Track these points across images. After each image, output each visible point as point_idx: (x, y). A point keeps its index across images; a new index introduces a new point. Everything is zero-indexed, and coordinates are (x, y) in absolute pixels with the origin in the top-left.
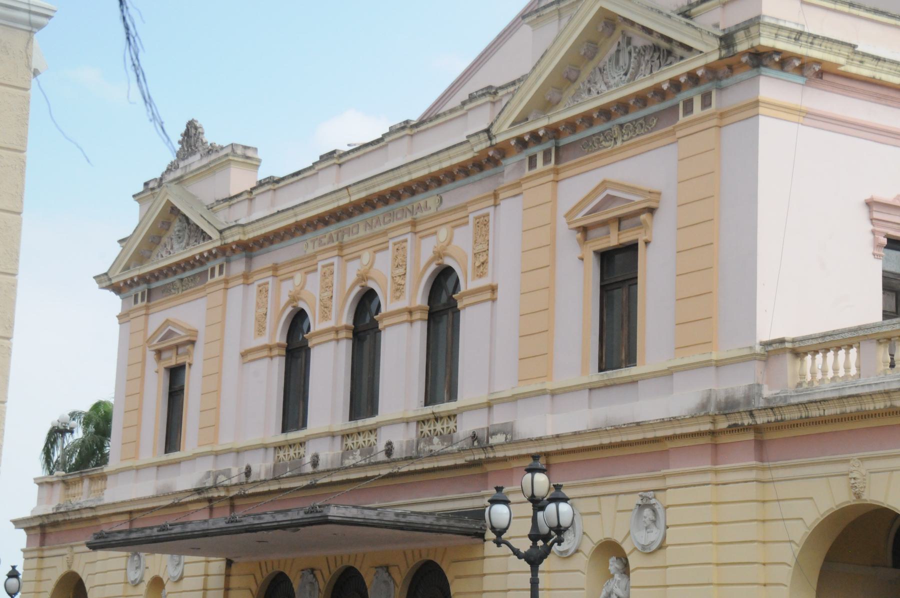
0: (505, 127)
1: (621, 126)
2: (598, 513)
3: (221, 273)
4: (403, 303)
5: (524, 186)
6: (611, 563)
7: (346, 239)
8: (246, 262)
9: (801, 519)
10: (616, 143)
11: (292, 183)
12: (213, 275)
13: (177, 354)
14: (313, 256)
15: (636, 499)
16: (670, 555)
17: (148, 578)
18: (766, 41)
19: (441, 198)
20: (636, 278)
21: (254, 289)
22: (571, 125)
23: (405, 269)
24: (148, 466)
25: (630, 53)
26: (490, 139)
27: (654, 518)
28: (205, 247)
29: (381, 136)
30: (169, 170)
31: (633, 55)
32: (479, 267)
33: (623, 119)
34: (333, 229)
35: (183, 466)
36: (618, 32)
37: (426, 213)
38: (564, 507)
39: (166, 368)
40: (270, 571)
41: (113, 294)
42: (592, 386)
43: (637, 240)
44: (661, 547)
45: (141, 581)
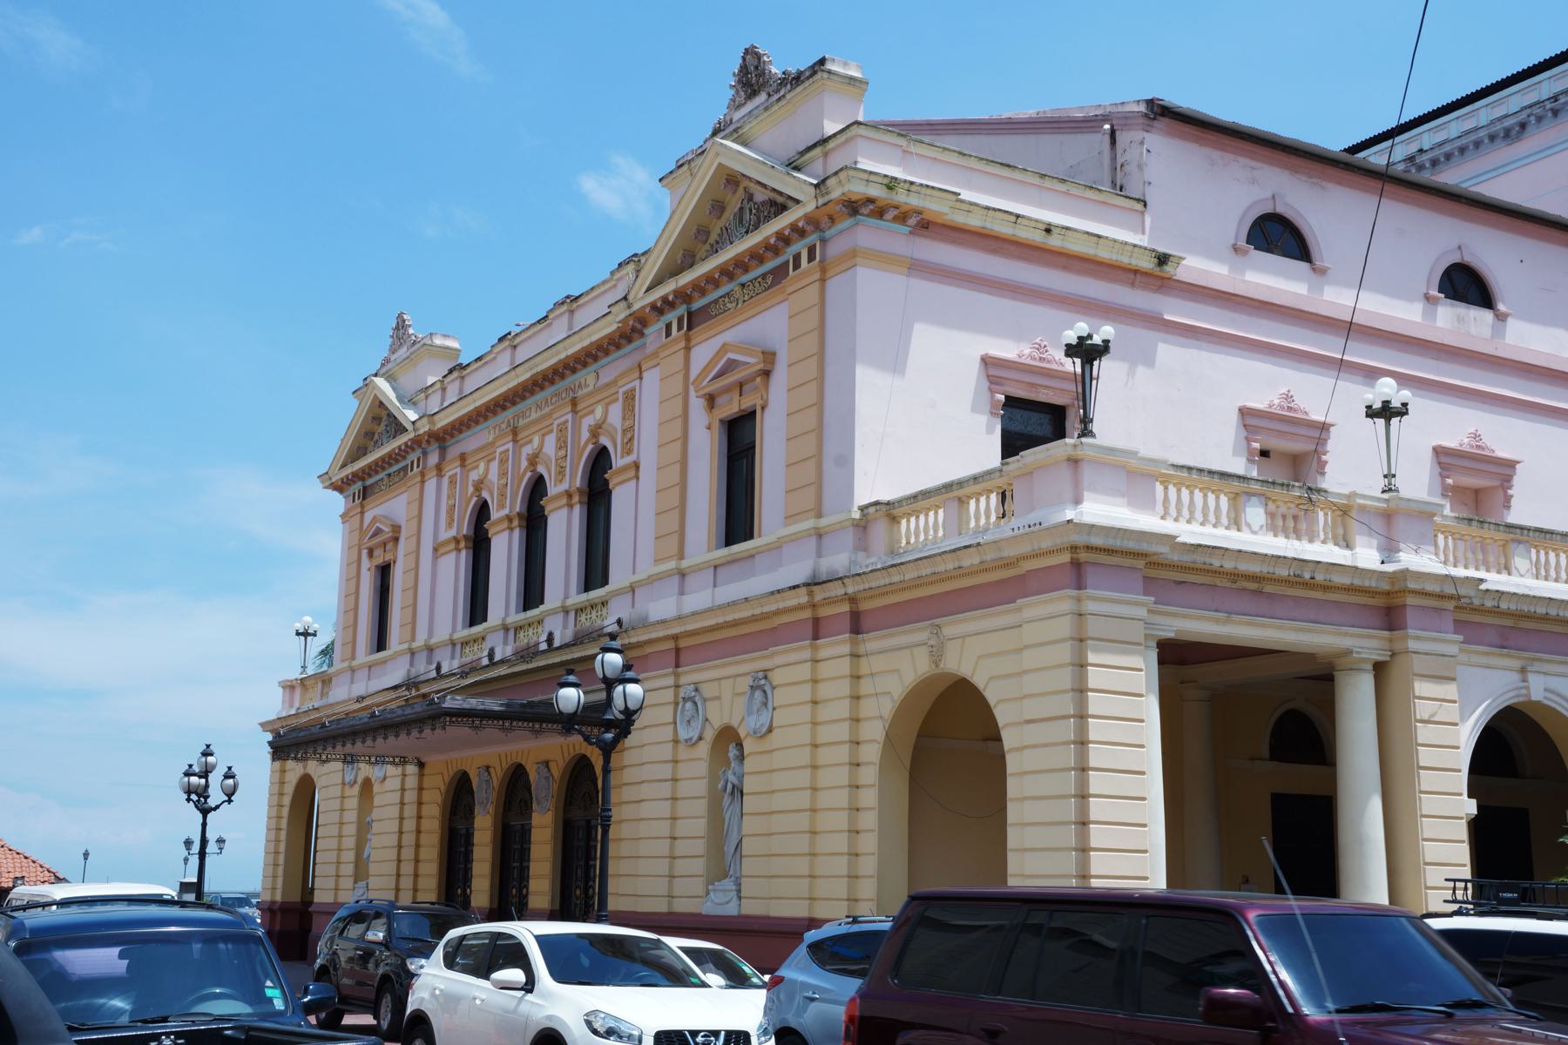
1: (743, 285)
2: (718, 698)
3: (418, 466)
4: (565, 486)
5: (662, 355)
6: (730, 749)
7: (522, 422)
8: (440, 454)
9: (889, 693)
10: (737, 304)
11: (477, 369)
12: (412, 470)
13: (385, 551)
14: (492, 444)
15: (749, 681)
16: (776, 739)
17: (360, 780)
18: (858, 189)
19: (598, 374)
20: (754, 447)
21: (445, 481)
22: (699, 288)
23: (567, 451)
24: (361, 667)
25: (751, 210)
26: (629, 307)
27: (764, 700)
28: (402, 440)
30: (383, 365)
31: (754, 211)
32: (627, 443)
33: (745, 278)
34: (510, 413)
36: (741, 190)
37: (585, 391)
38: (634, 689)
40: (455, 770)
41: (336, 494)
42: (718, 562)
43: (755, 405)
44: (770, 730)
45: (355, 782)
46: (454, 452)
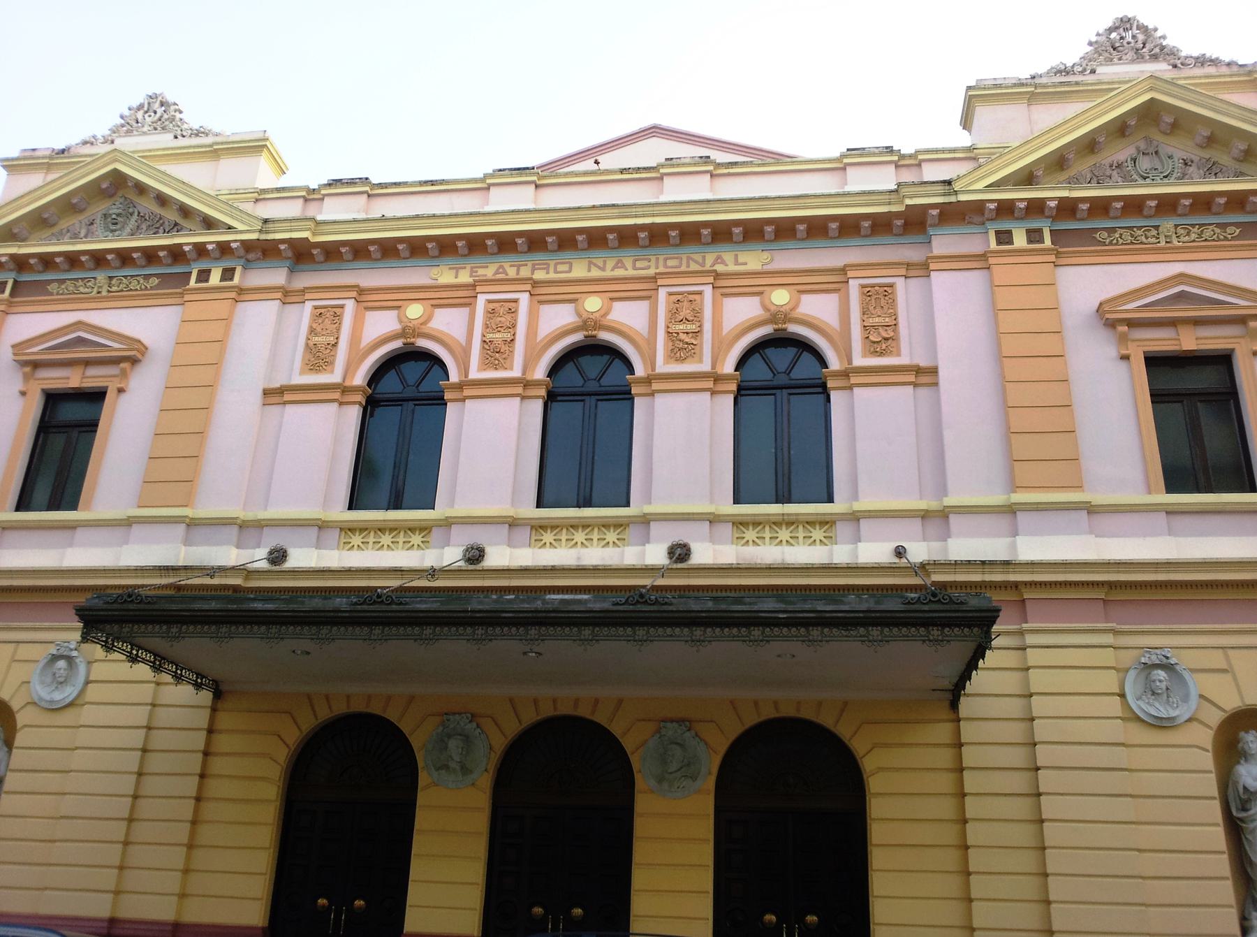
0: (980, 185)
19: (772, 260)
29: (656, 165)
35: (80, 534)
39: (43, 390)
46: (306, 280)
